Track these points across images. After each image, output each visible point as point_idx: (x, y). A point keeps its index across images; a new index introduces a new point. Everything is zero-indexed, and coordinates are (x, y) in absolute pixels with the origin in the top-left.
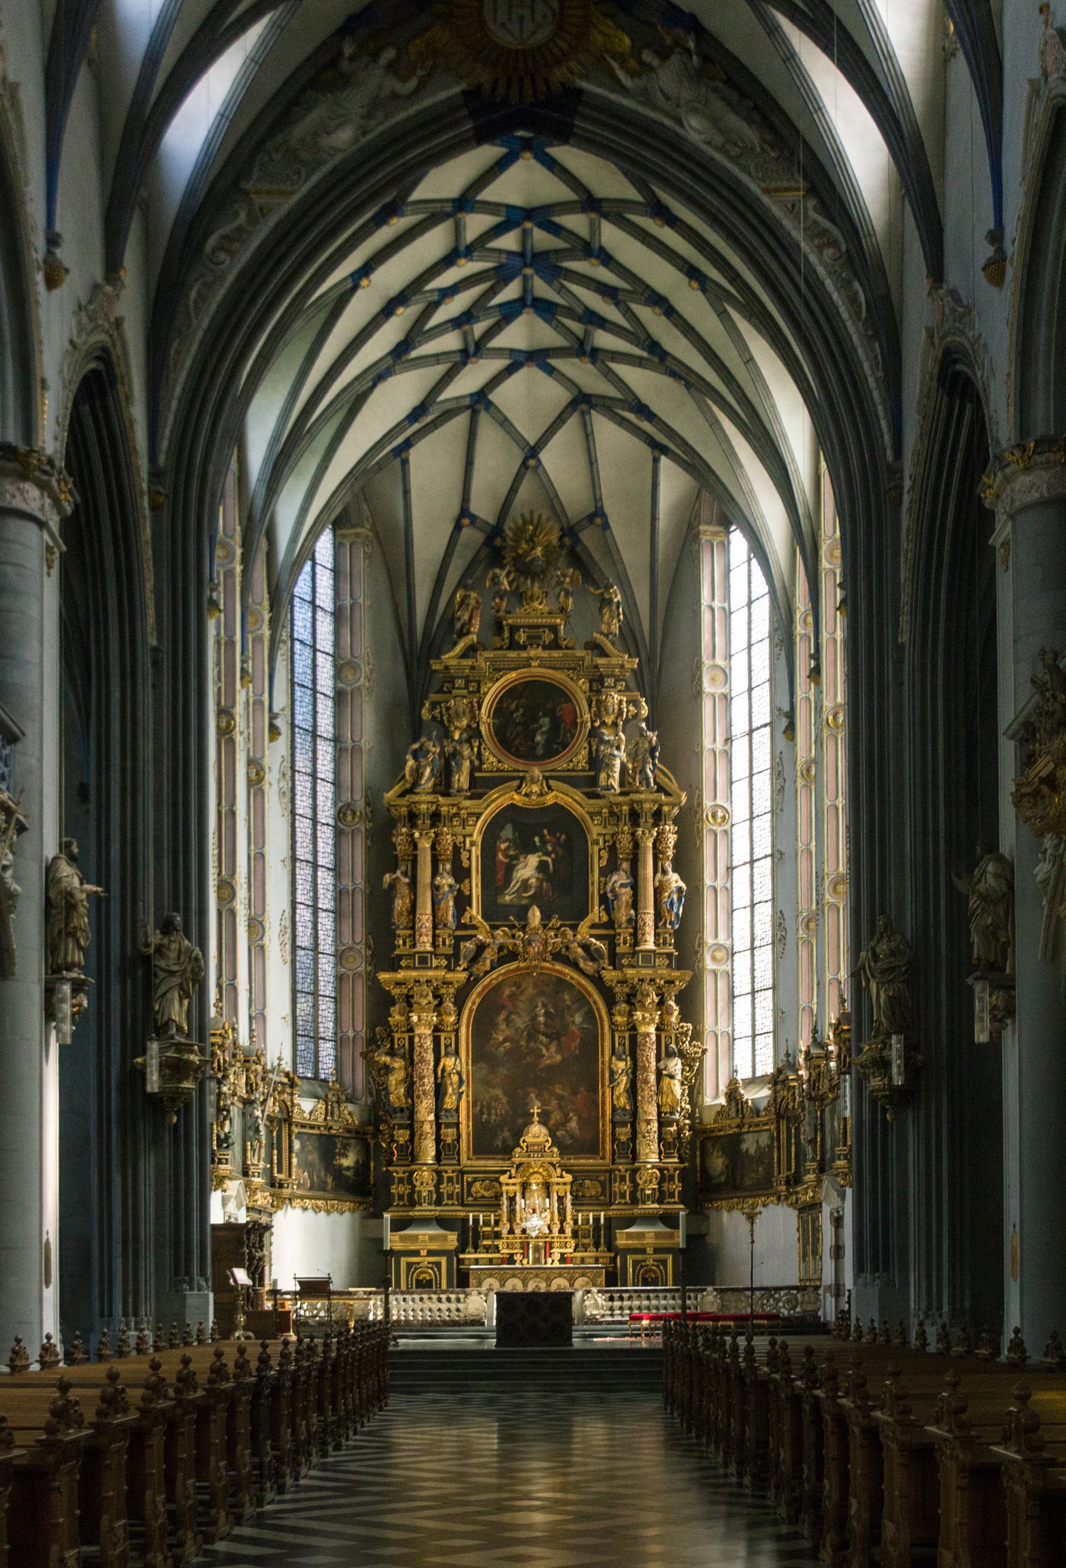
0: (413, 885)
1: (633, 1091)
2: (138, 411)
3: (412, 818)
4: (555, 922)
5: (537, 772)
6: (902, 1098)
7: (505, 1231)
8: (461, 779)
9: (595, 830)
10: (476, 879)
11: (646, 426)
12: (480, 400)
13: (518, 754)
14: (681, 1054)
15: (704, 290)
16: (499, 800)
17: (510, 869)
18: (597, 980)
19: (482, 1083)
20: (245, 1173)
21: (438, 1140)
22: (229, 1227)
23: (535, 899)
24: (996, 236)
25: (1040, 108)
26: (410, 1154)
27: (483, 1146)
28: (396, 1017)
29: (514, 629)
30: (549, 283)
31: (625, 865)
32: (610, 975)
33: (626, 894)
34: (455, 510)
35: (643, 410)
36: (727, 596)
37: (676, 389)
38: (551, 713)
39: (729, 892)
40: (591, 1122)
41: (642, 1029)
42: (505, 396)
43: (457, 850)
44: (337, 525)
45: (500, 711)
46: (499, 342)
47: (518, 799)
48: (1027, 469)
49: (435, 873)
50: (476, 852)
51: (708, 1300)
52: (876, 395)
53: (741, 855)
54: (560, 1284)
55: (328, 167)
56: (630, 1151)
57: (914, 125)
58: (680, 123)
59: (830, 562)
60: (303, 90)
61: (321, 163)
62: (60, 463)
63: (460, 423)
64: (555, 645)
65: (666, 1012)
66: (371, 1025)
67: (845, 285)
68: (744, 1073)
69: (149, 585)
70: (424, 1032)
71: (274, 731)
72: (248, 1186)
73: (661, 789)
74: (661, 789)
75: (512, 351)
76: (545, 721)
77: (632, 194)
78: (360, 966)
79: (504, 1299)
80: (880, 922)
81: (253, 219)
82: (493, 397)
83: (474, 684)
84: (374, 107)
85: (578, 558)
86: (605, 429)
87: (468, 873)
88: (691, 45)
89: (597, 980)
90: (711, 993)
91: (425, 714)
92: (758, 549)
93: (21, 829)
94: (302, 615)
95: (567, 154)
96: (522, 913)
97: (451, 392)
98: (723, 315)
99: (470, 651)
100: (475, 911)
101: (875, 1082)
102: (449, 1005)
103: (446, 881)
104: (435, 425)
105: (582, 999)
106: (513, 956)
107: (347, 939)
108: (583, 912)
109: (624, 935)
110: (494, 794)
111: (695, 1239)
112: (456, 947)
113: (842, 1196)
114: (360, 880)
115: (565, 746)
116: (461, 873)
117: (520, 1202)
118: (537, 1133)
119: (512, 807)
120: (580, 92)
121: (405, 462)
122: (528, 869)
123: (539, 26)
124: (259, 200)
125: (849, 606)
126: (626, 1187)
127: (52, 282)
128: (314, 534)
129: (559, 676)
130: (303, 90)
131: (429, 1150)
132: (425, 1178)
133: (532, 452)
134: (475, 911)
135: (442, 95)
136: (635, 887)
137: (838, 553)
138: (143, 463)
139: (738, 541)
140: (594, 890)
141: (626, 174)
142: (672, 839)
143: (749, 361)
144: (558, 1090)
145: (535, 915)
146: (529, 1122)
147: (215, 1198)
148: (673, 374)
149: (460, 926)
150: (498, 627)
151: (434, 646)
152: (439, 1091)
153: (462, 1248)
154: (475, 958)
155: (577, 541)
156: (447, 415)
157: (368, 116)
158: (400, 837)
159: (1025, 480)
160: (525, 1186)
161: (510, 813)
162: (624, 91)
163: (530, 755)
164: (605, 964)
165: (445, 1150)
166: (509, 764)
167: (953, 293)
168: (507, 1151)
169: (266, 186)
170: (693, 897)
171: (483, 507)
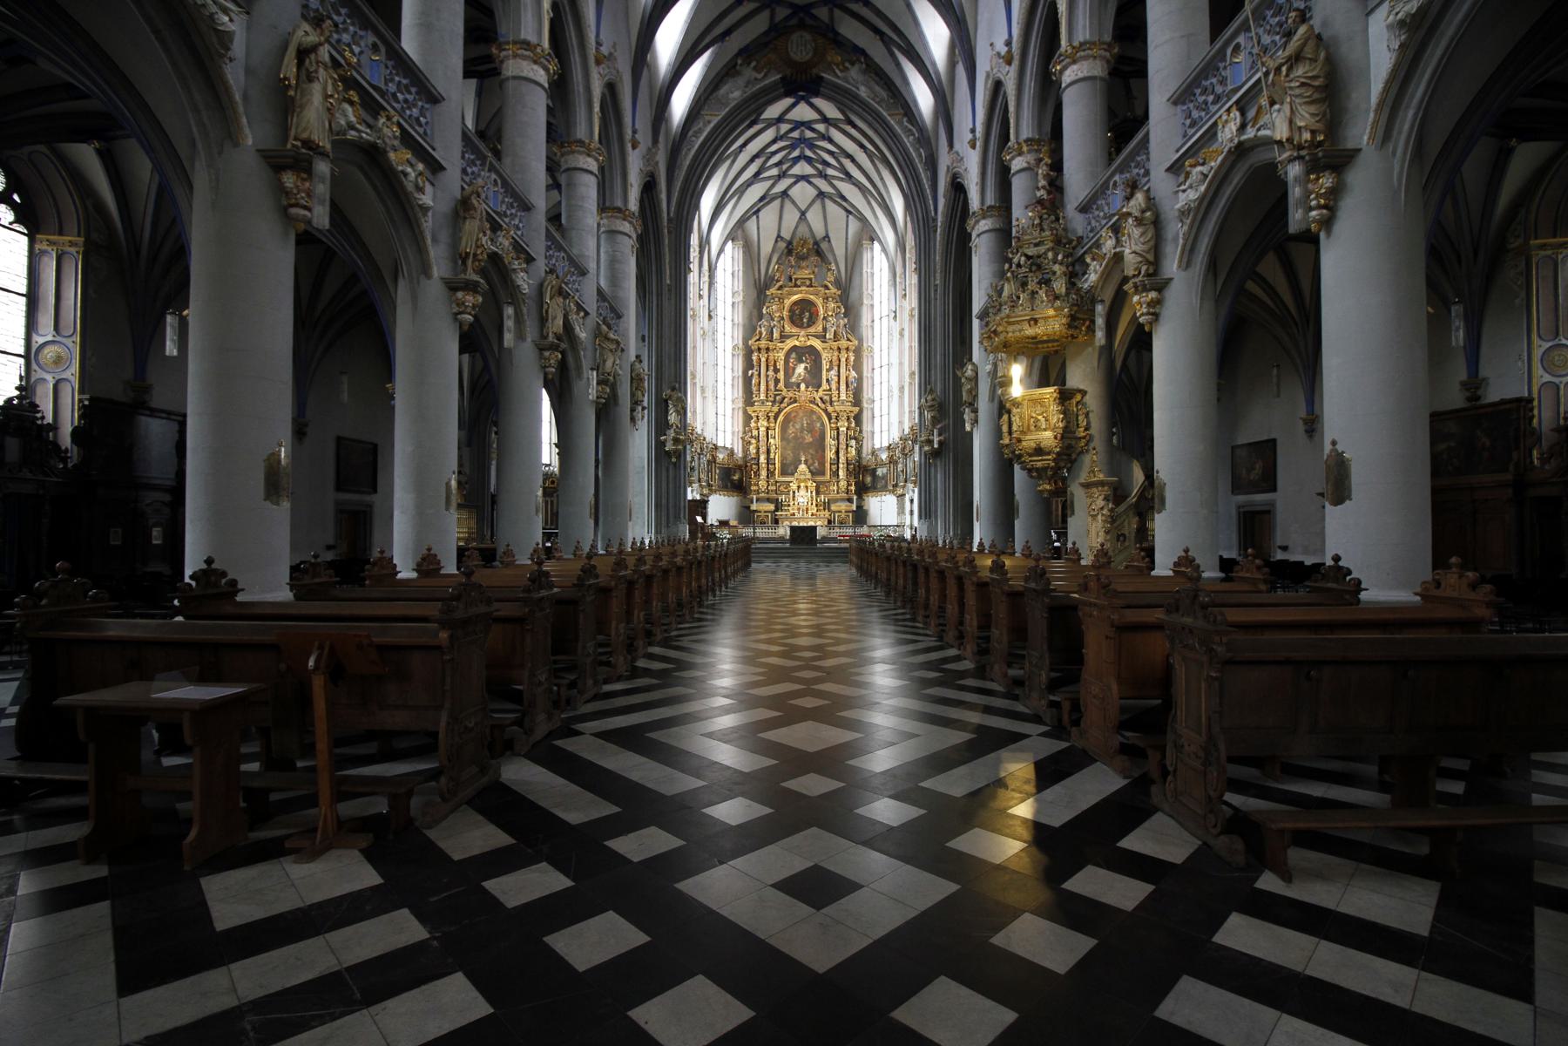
0: (759, 375)
1: (837, 452)
2: (663, 196)
3: (759, 349)
4: (810, 389)
5: (803, 333)
6: (936, 454)
7: (791, 503)
8: (776, 335)
9: (825, 356)
10: (782, 373)
11: (844, 204)
12: (785, 194)
13: (797, 326)
14: (855, 438)
15: (866, 152)
16: (790, 343)
17: (794, 369)
18: (826, 411)
19: (784, 448)
20: (699, 481)
21: (768, 470)
22: (694, 501)
23: (803, 380)
24: (973, 131)
25: (990, 82)
26: (757, 474)
27: (784, 473)
28: (753, 425)
29: (796, 279)
30: (810, 149)
31: (836, 368)
32: (830, 409)
33: (836, 379)
34: (775, 236)
35: (843, 198)
36: (872, 268)
37: (855, 190)
38: (809, 311)
39: (872, 378)
40: (822, 464)
41: (841, 429)
42: (793, 192)
43: (775, 362)
44: (733, 240)
45: (790, 311)
46: (790, 172)
47: (797, 343)
48: (984, 218)
49: (767, 370)
50: (782, 362)
51: (864, 530)
52: (928, 191)
53: (877, 365)
54: (811, 523)
55: (732, 105)
56: (836, 474)
57: (944, 91)
58: (858, 89)
59: (911, 255)
60: (722, 78)
61: (729, 104)
62: (637, 214)
63: (777, 203)
64: (811, 286)
65: (850, 423)
66: (744, 428)
67: (917, 150)
68: (877, 446)
69: (667, 261)
70: (762, 429)
71: (710, 317)
72: (701, 486)
73: (848, 340)
74: (848, 340)
75: (796, 176)
76: (807, 314)
77: (840, 116)
78: (741, 405)
79: (793, 529)
80: (929, 387)
81: (705, 125)
82: (790, 193)
83: (781, 299)
84: (748, 83)
85: (819, 253)
86: (828, 203)
87: (779, 370)
88: (863, 60)
89: (826, 411)
90: (866, 416)
91: (764, 312)
92: (884, 250)
93: (623, 350)
94: (719, 273)
95: (818, 101)
96: (798, 386)
97: (774, 191)
98: (872, 162)
99: (780, 288)
100: (781, 385)
101: (926, 448)
102: (772, 420)
103: (771, 373)
104: (768, 203)
105: (820, 418)
106: (795, 401)
107: (736, 395)
108: (819, 386)
109: (835, 393)
110: (788, 341)
111: (860, 507)
112: (775, 398)
113: (913, 491)
114: (740, 373)
115: (814, 323)
116: (776, 371)
117: (797, 494)
118: (803, 467)
119: (795, 346)
120: (822, 78)
121: (758, 217)
122: (800, 369)
123: (807, 54)
124: (707, 118)
125: (918, 270)
126: (835, 488)
127: (634, 147)
128: (724, 243)
129: (812, 297)
130: (722, 78)
131: (764, 473)
132: (762, 484)
133: (803, 214)
134: (781, 385)
135: (773, 79)
136: (839, 376)
137: (914, 251)
138: (665, 215)
139: (876, 245)
140: (824, 377)
141: (838, 109)
142: (852, 358)
143: (882, 179)
144: (811, 451)
145: (803, 386)
146: (800, 463)
147: (689, 489)
148: (854, 184)
149: (776, 390)
150: (791, 280)
151: (767, 287)
152: (768, 452)
153: (777, 510)
154: (781, 402)
155: (819, 246)
156: (773, 199)
157: (746, 87)
158: (754, 358)
159: (983, 222)
160: (799, 487)
161: (794, 348)
162: (838, 77)
163: (801, 326)
164: (828, 404)
165: (770, 474)
166: (795, 330)
167: (957, 153)
168: (793, 474)
169: (709, 113)
170: (860, 380)
171: (786, 235)
